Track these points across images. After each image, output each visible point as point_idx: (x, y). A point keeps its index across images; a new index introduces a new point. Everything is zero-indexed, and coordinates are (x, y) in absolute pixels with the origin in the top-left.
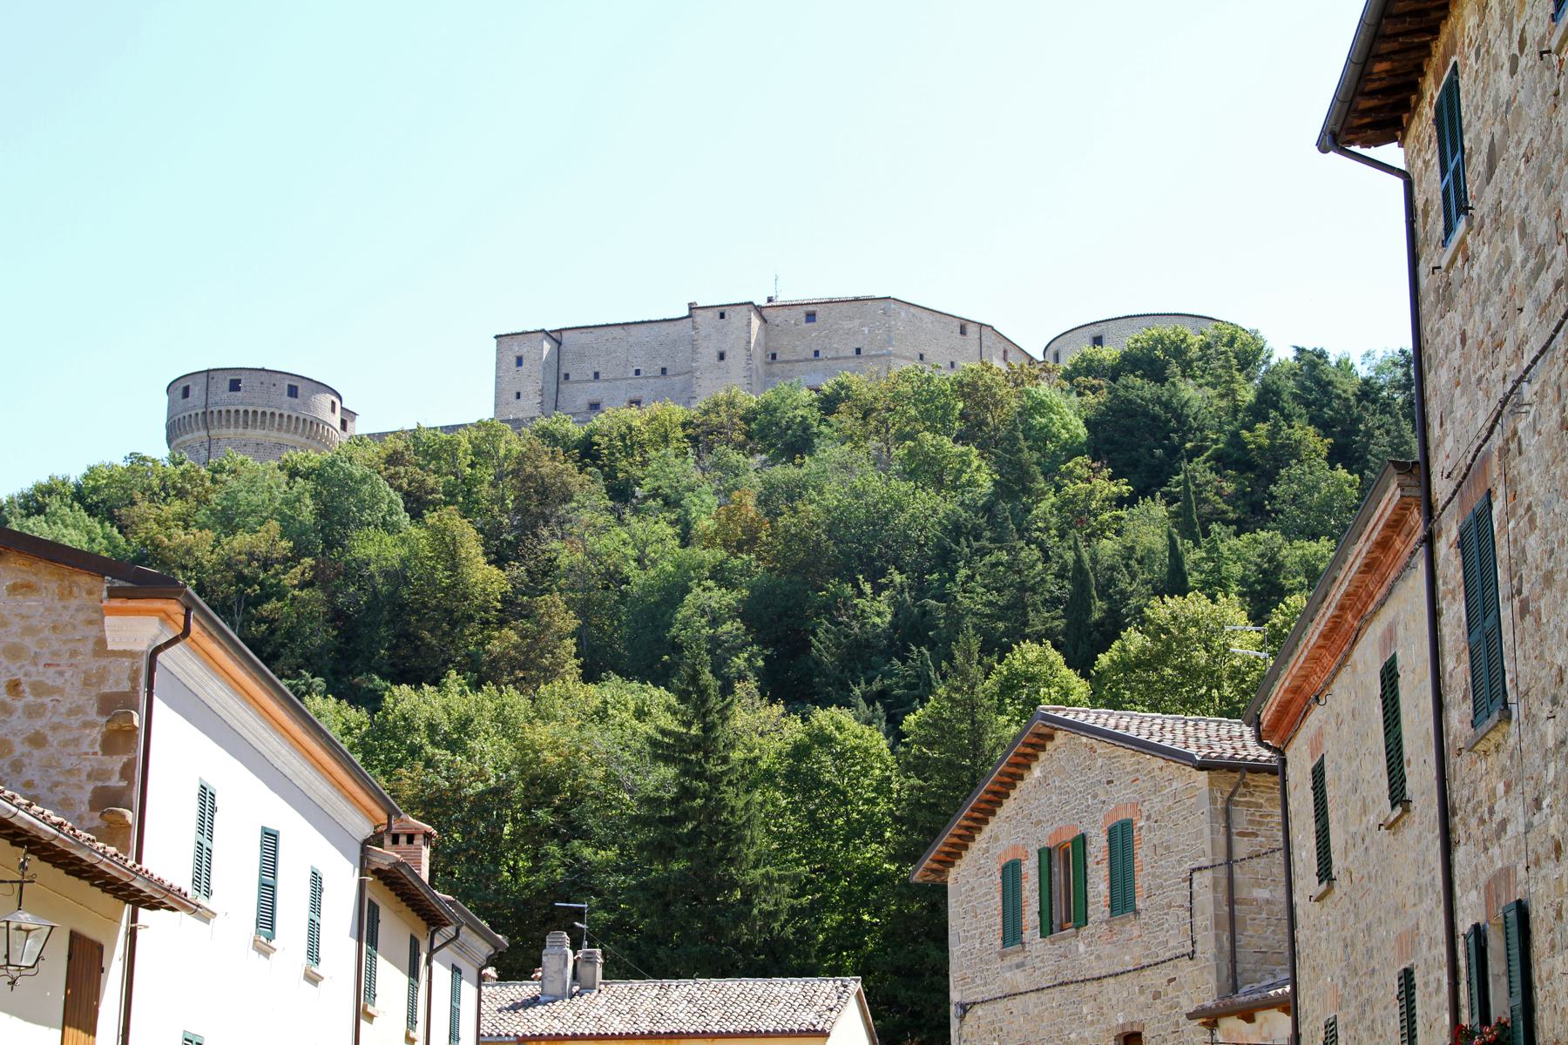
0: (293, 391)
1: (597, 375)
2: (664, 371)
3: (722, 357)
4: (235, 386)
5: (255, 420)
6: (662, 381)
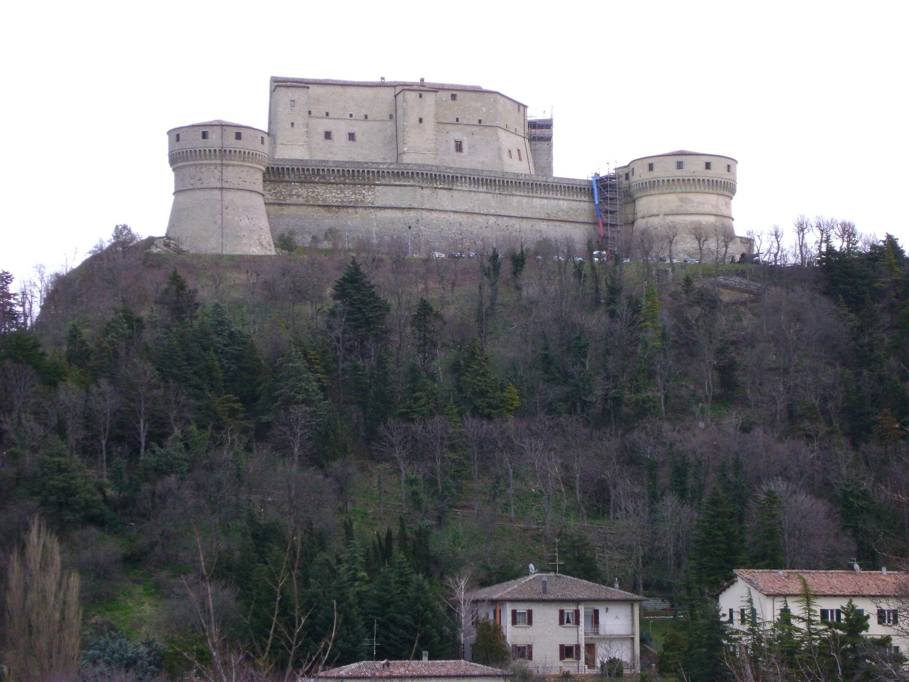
1: (327, 114)
2: (366, 117)
3: (421, 120)
4: (238, 136)
5: (248, 158)
6: (365, 124)
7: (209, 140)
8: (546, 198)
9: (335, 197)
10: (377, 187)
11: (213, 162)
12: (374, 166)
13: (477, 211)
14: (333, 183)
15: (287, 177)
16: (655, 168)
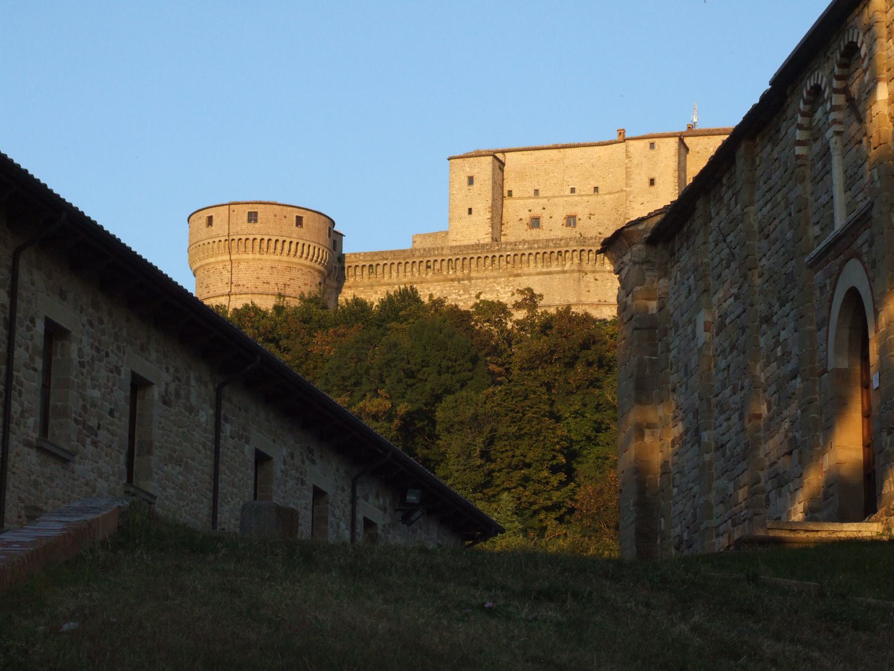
0: (299, 221)
1: (536, 191)
2: (596, 189)
3: (652, 182)
4: (253, 217)
6: (594, 199)
7: (213, 228)
10: (518, 279)
11: (220, 258)
12: (509, 247)
14: (452, 280)
15: (387, 276)
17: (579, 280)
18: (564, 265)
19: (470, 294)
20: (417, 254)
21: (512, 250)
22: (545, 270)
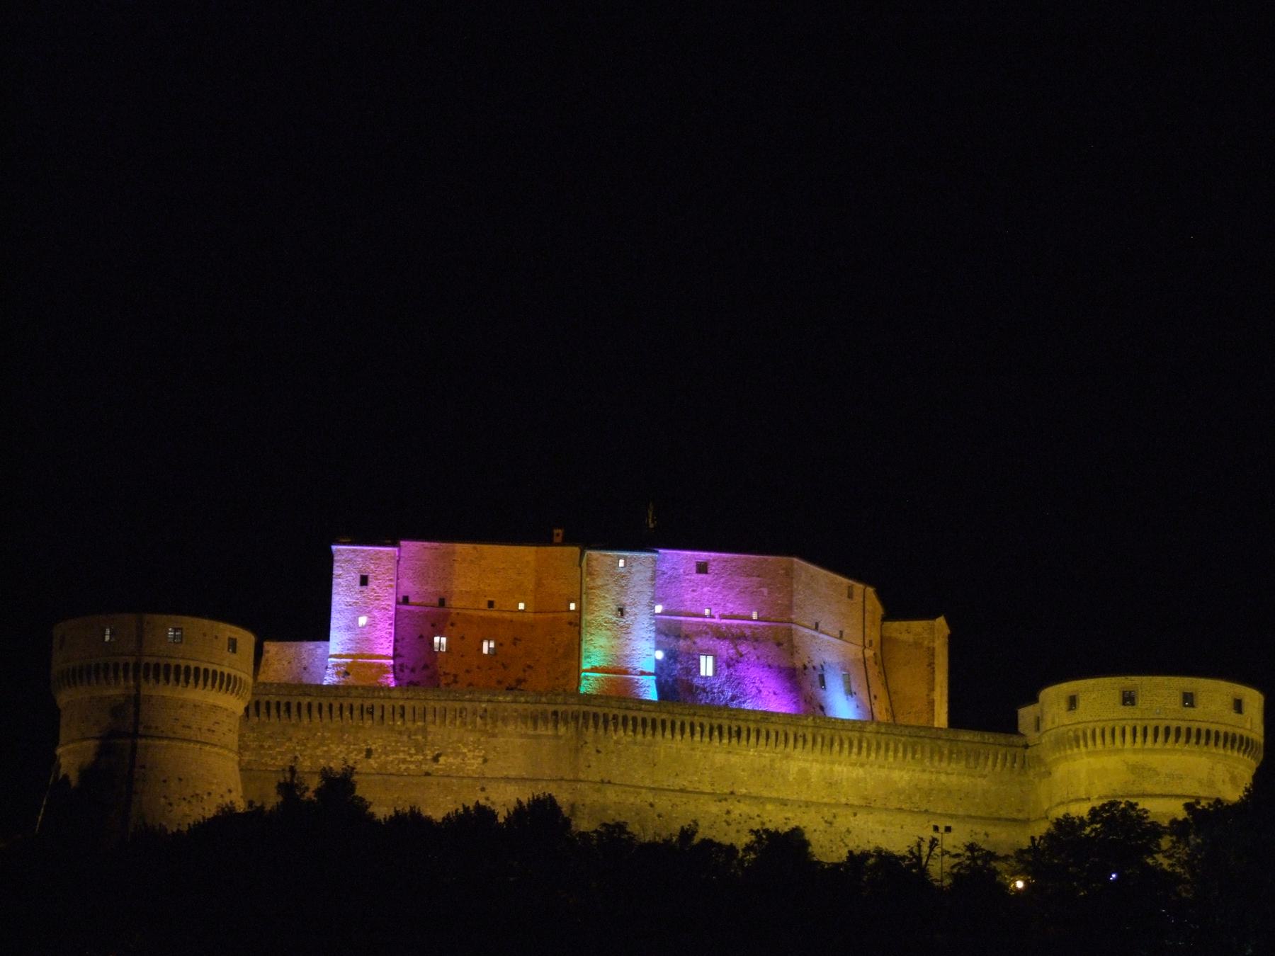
8: (862, 765)
9: (404, 761)
10: (493, 740)
13: (708, 789)
16: (1081, 704)
17: (577, 750)
18: (556, 727)
19: (425, 755)
20: (354, 693)
21: (489, 701)
22: (531, 732)
